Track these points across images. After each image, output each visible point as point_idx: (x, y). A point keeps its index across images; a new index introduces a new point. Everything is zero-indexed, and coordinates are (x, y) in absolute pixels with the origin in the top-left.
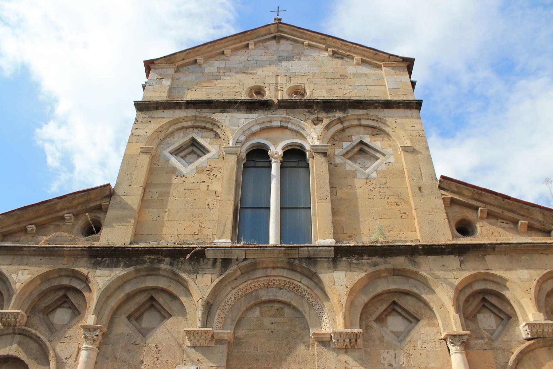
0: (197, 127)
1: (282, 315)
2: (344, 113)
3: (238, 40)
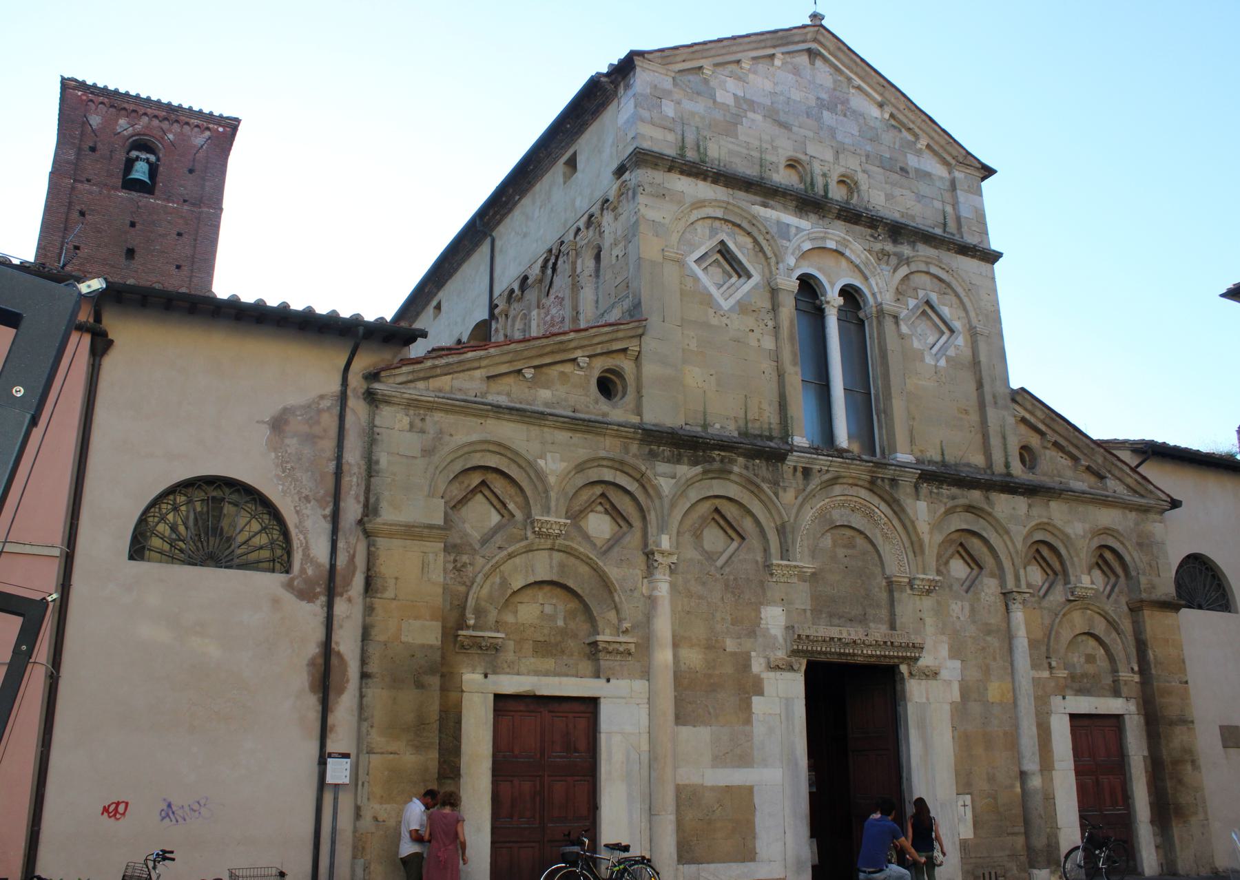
0: (726, 221)
1: (854, 547)
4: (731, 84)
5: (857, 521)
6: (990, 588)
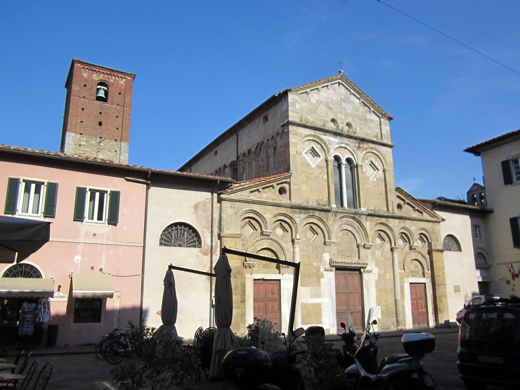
4: (315, 96)
5: (350, 228)
6: (388, 246)
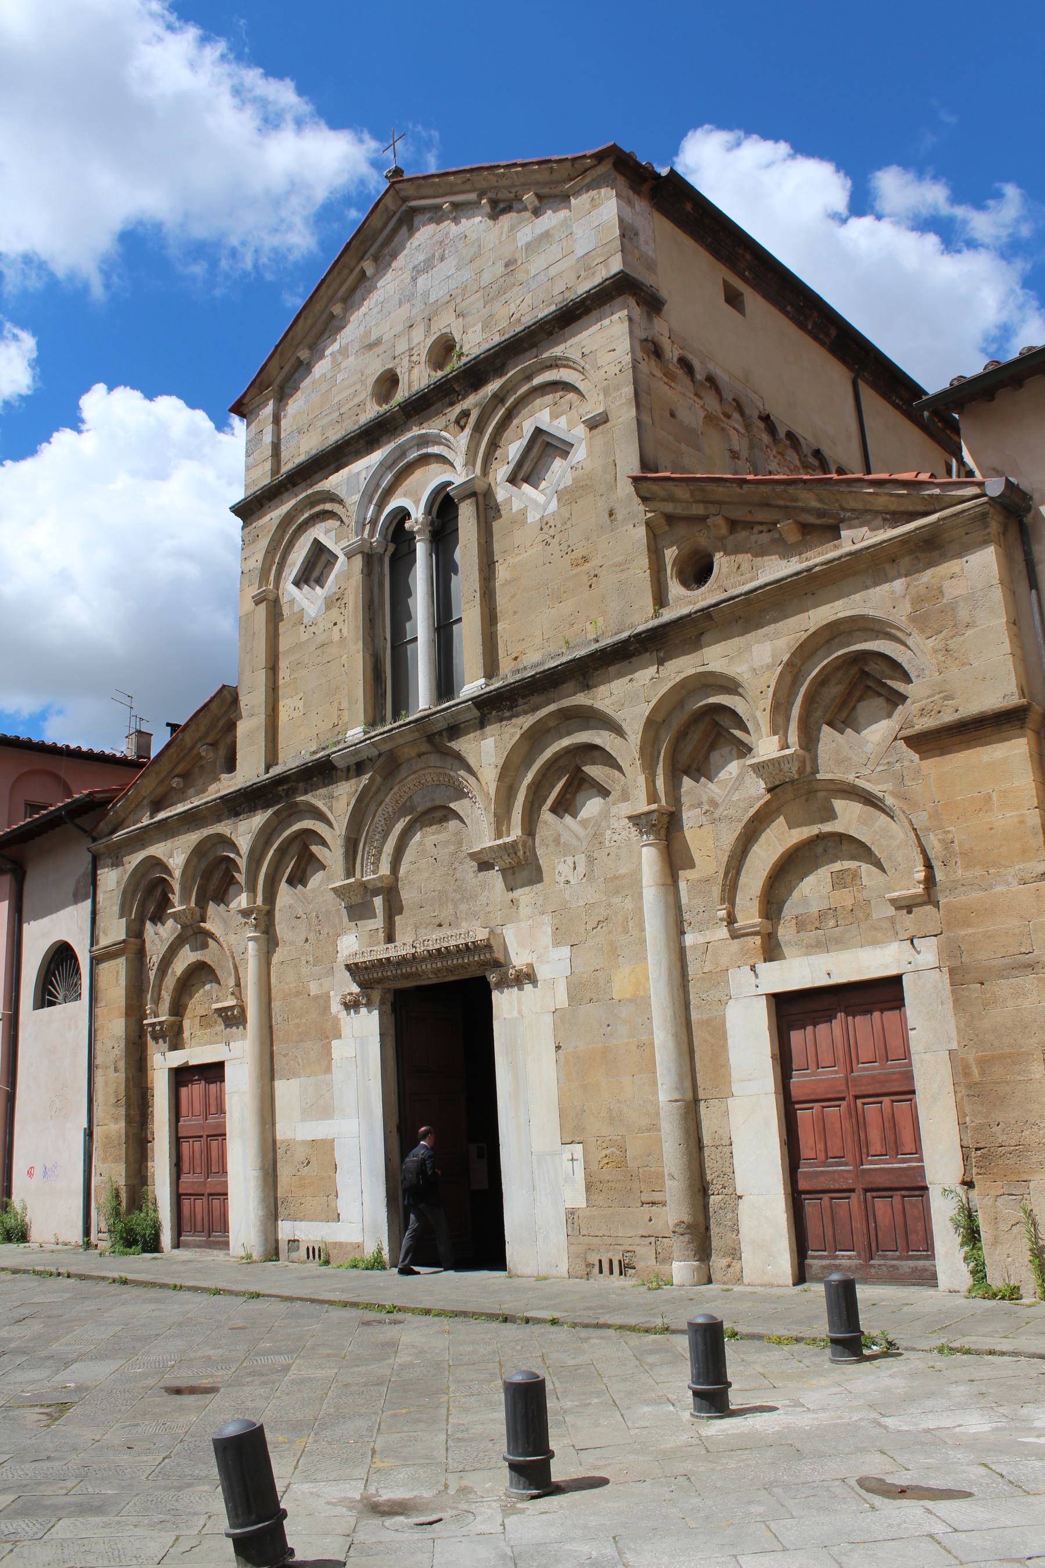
2: (501, 376)
3: (346, 271)
